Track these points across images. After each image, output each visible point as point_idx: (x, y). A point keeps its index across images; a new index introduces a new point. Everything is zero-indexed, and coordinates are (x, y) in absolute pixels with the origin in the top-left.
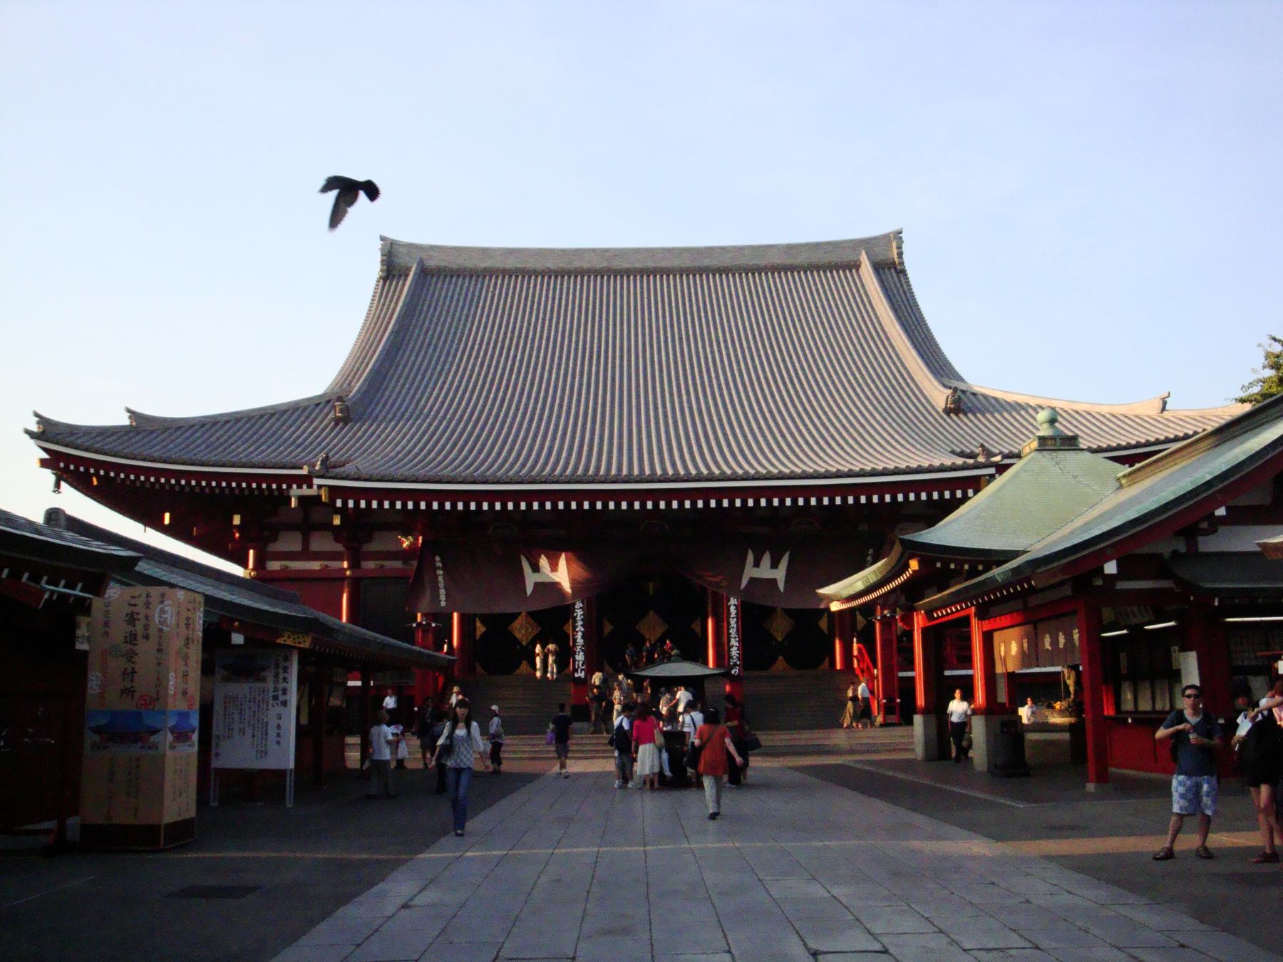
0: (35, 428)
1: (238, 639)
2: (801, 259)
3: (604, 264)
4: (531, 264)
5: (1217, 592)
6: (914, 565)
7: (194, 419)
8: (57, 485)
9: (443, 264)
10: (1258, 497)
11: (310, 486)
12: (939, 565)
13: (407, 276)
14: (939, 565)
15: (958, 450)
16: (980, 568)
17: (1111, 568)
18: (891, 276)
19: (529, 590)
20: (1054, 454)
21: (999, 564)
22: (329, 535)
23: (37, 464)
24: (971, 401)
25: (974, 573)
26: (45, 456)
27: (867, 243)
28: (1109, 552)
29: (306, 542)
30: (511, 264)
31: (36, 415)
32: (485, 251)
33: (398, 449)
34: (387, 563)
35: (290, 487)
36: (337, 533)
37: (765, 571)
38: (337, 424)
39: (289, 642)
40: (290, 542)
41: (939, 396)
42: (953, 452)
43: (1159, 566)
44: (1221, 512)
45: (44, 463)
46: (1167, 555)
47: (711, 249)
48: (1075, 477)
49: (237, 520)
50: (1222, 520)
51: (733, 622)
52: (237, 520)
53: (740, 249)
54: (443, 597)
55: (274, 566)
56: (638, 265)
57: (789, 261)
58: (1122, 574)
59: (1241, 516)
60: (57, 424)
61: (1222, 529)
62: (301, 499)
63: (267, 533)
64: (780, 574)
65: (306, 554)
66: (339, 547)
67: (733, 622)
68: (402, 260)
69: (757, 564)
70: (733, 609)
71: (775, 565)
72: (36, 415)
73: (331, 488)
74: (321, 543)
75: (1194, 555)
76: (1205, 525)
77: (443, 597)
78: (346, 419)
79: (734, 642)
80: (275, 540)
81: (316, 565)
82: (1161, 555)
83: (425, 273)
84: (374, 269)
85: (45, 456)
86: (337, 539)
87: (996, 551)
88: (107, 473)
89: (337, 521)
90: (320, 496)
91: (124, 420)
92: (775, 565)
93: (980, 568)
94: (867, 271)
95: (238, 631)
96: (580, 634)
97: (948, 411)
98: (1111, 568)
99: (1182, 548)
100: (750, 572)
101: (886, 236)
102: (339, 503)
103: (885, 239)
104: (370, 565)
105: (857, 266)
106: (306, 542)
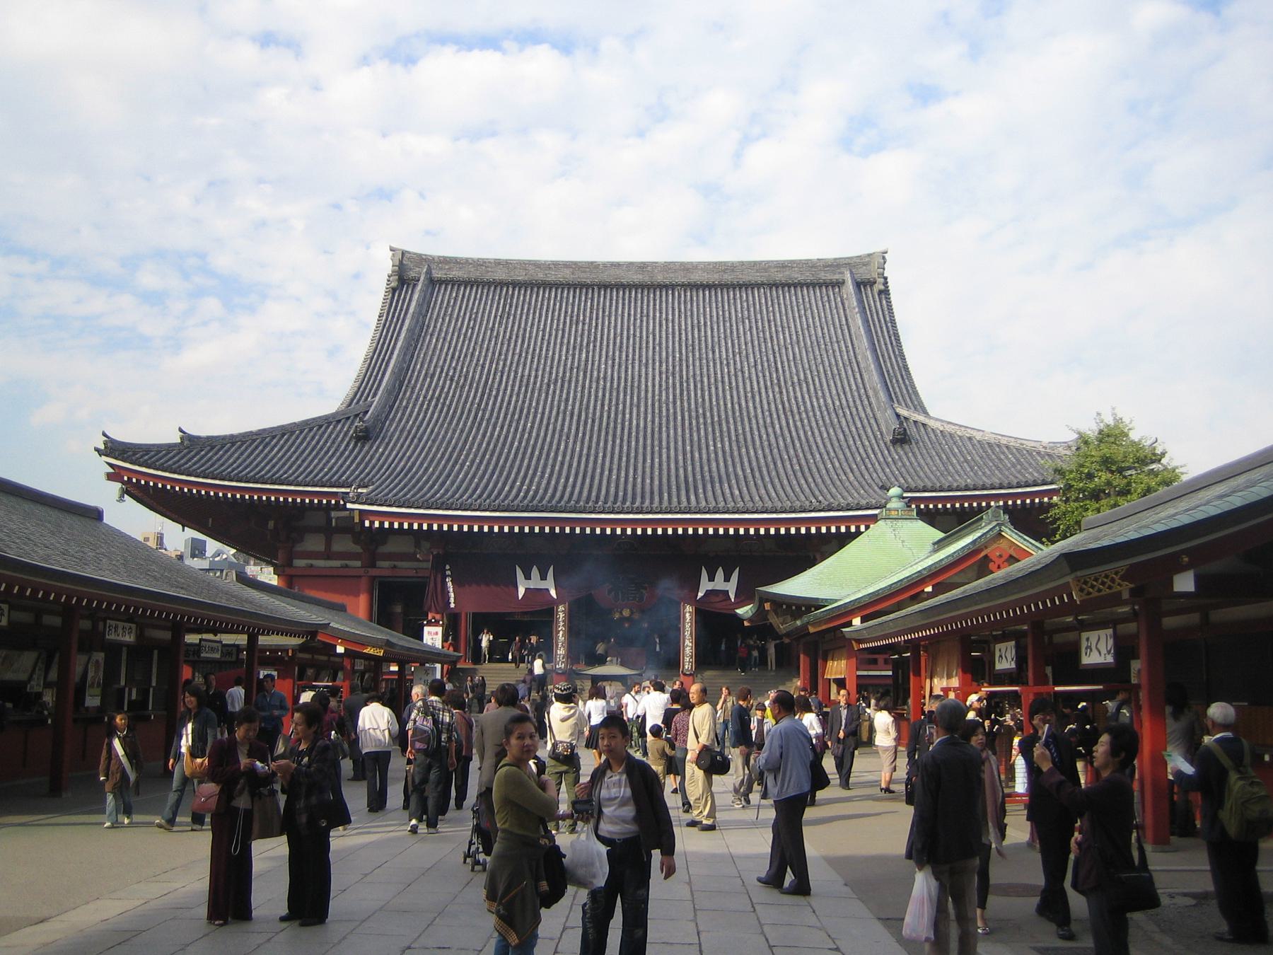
1: (340, 649)
6: (767, 606)
8: (121, 499)
13: (415, 286)
17: (857, 621)
19: (521, 592)
23: (104, 477)
26: (111, 470)
27: (849, 264)
29: (328, 544)
37: (719, 583)
39: (372, 652)
40: (314, 543)
41: (888, 425)
44: (929, 589)
45: (110, 477)
49: (271, 524)
52: (271, 524)
54: (452, 600)
55: (300, 563)
62: (337, 519)
64: (731, 587)
65: (328, 555)
66: (358, 549)
67: (687, 626)
69: (711, 579)
71: (727, 579)
72: (104, 435)
73: (360, 511)
74: (343, 544)
77: (452, 600)
78: (364, 437)
79: (687, 642)
80: (302, 540)
81: (337, 563)
83: (432, 282)
85: (111, 470)
91: (176, 438)
92: (727, 579)
94: (850, 287)
95: (341, 644)
97: (895, 442)
100: (705, 586)
101: (869, 255)
102: (367, 524)
105: (839, 284)
106: (328, 544)
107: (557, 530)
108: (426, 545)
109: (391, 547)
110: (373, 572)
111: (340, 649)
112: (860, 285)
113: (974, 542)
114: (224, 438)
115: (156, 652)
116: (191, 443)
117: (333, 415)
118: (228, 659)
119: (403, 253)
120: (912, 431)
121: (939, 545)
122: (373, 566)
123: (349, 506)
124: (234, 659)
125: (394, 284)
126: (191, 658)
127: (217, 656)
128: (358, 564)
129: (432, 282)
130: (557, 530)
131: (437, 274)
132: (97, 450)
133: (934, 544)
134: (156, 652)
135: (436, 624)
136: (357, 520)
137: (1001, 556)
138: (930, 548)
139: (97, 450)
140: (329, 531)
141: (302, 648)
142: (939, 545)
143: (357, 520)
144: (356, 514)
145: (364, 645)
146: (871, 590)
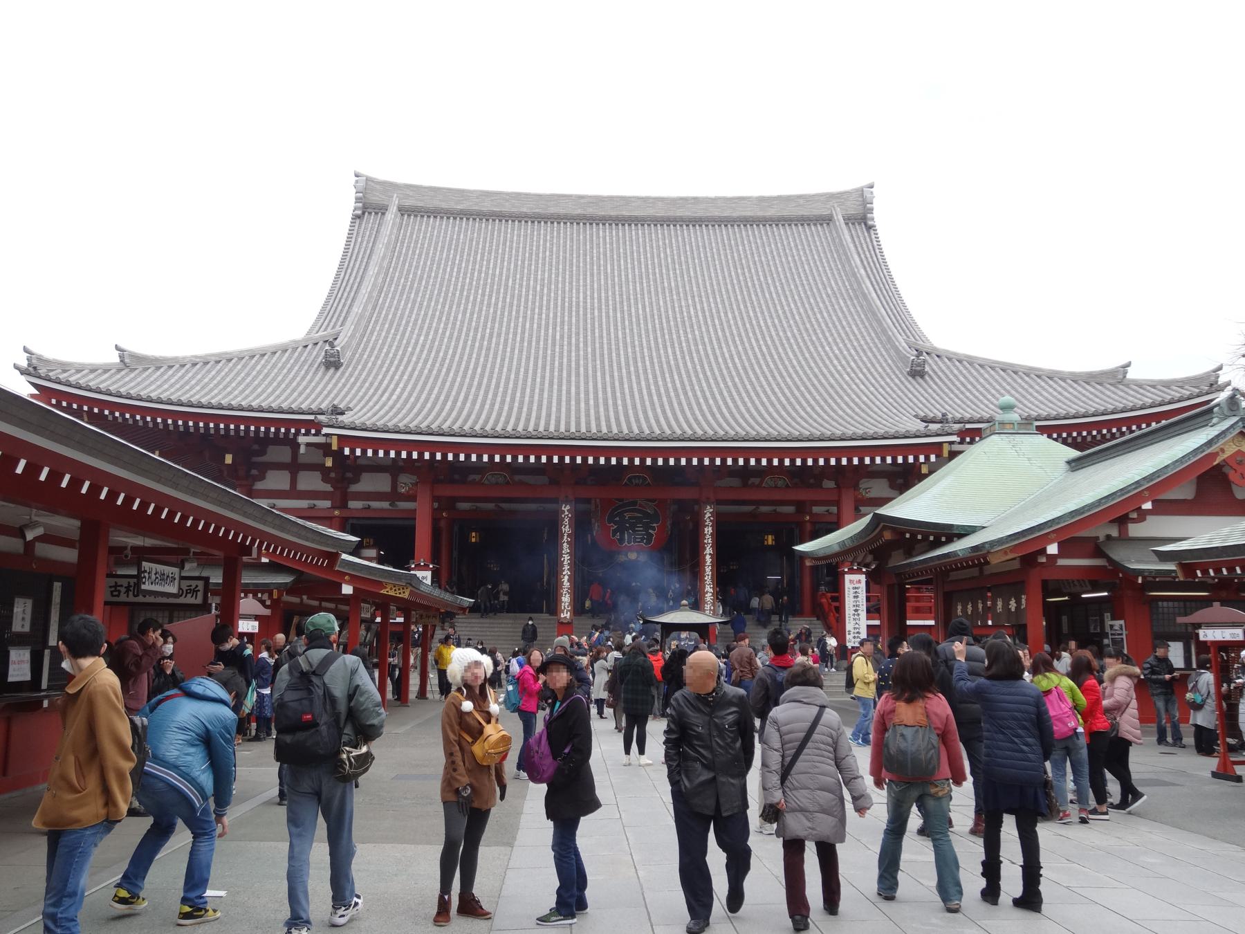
0: (24, 364)
1: (347, 589)
2: (771, 212)
3: (579, 211)
4: (507, 208)
5: (1140, 572)
7: (184, 358)
9: (420, 204)
10: (1185, 492)
11: (318, 433)
12: (908, 536)
14: (908, 536)
15: (922, 414)
16: (943, 539)
17: (1053, 549)
18: (860, 230)
20: (1012, 437)
21: (961, 536)
22: (317, 475)
24: (936, 363)
25: (938, 544)
28: (1053, 536)
29: (294, 482)
30: (487, 206)
31: (26, 350)
32: (462, 193)
33: (394, 397)
34: (375, 504)
35: (298, 433)
36: (325, 473)
38: (327, 368)
39: (392, 593)
40: (277, 480)
42: (916, 416)
43: (1096, 548)
44: (1148, 506)
46: (1102, 539)
47: (685, 199)
48: (1029, 459)
49: (229, 459)
50: (1148, 512)
51: (708, 570)
52: (229, 459)
53: (713, 201)
56: (613, 213)
57: (760, 214)
58: (1063, 553)
59: (1165, 508)
60: (47, 362)
61: (1149, 518)
62: (308, 445)
63: (254, 472)
65: (293, 493)
66: (328, 488)
67: (708, 570)
68: (376, 198)
70: (708, 558)
72: (26, 350)
74: (310, 481)
75: (1124, 538)
76: (1134, 515)
78: (332, 363)
80: (262, 477)
82: (1097, 538)
84: (347, 205)
86: (326, 479)
87: (958, 526)
88: (101, 411)
89: (329, 463)
90: (330, 445)
93: (943, 539)
95: (348, 583)
96: (566, 577)
98: (1053, 549)
99: (1115, 533)
102: (347, 451)
103: (860, 192)
104: (353, 504)
106: (294, 482)
107: (567, 460)
108: (406, 482)
109: (368, 483)
110: (346, 514)
111: (347, 589)
112: (849, 220)
113: (1210, 443)
114: (176, 359)
115: (57, 586)
116: (129, 361)
117: (295, 342)
118: (190, 600)
119: (368, 179)
120: (931, 365)
121: (1075, 465)
122: (343, 505)
123: (325, 431)
124: (199, 600)
125: (359, 212)
126: (123, 598)
127: (173, 589)
128: (328, 504)
129: (403, 211)
130: (567, 460)
131: (408, 203)
132: (16, 367)
133: (1069, 462)
134: (57, 586)
135: (426, 568)
136: (335, 447)
137: (1240, 463)
138: (1064, 467)
139: (16, 367)
140: (294, 467)
141: (291, 589)
142: (1075, 465)
143: (335, 447)
144: (335, 438)
145: (381, 585)
146: (1072, 506)
